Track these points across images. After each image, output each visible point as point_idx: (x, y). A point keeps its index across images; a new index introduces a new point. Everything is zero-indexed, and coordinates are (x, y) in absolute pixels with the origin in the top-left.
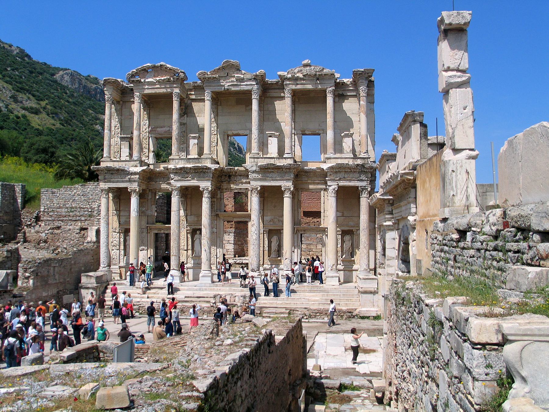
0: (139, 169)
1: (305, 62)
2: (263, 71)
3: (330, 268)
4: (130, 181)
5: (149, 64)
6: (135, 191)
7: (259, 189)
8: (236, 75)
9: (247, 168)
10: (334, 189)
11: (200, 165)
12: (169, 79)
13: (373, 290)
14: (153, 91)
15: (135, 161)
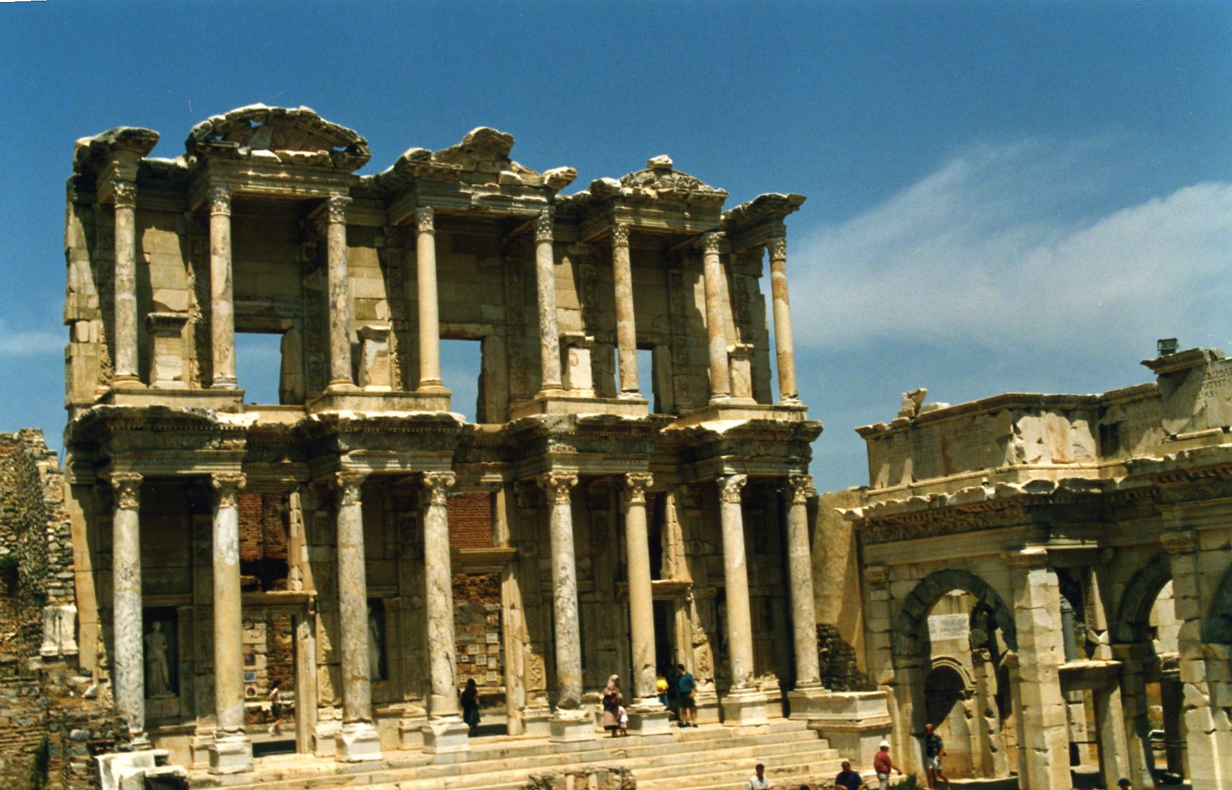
0: (244, 420)
1: (663, 159)
2: (573, 169)
3: (744, 683)
4: (216, 458)
5: (260, 106)
6: (230, 487)
7: (575, 482)
8: (504, 173)
9: (548, 425)
10: (738, 484)
11: (433, 413)
12: (325, 158)
13: (882, 723)
14: (273, 189)
15: (231, 394)
